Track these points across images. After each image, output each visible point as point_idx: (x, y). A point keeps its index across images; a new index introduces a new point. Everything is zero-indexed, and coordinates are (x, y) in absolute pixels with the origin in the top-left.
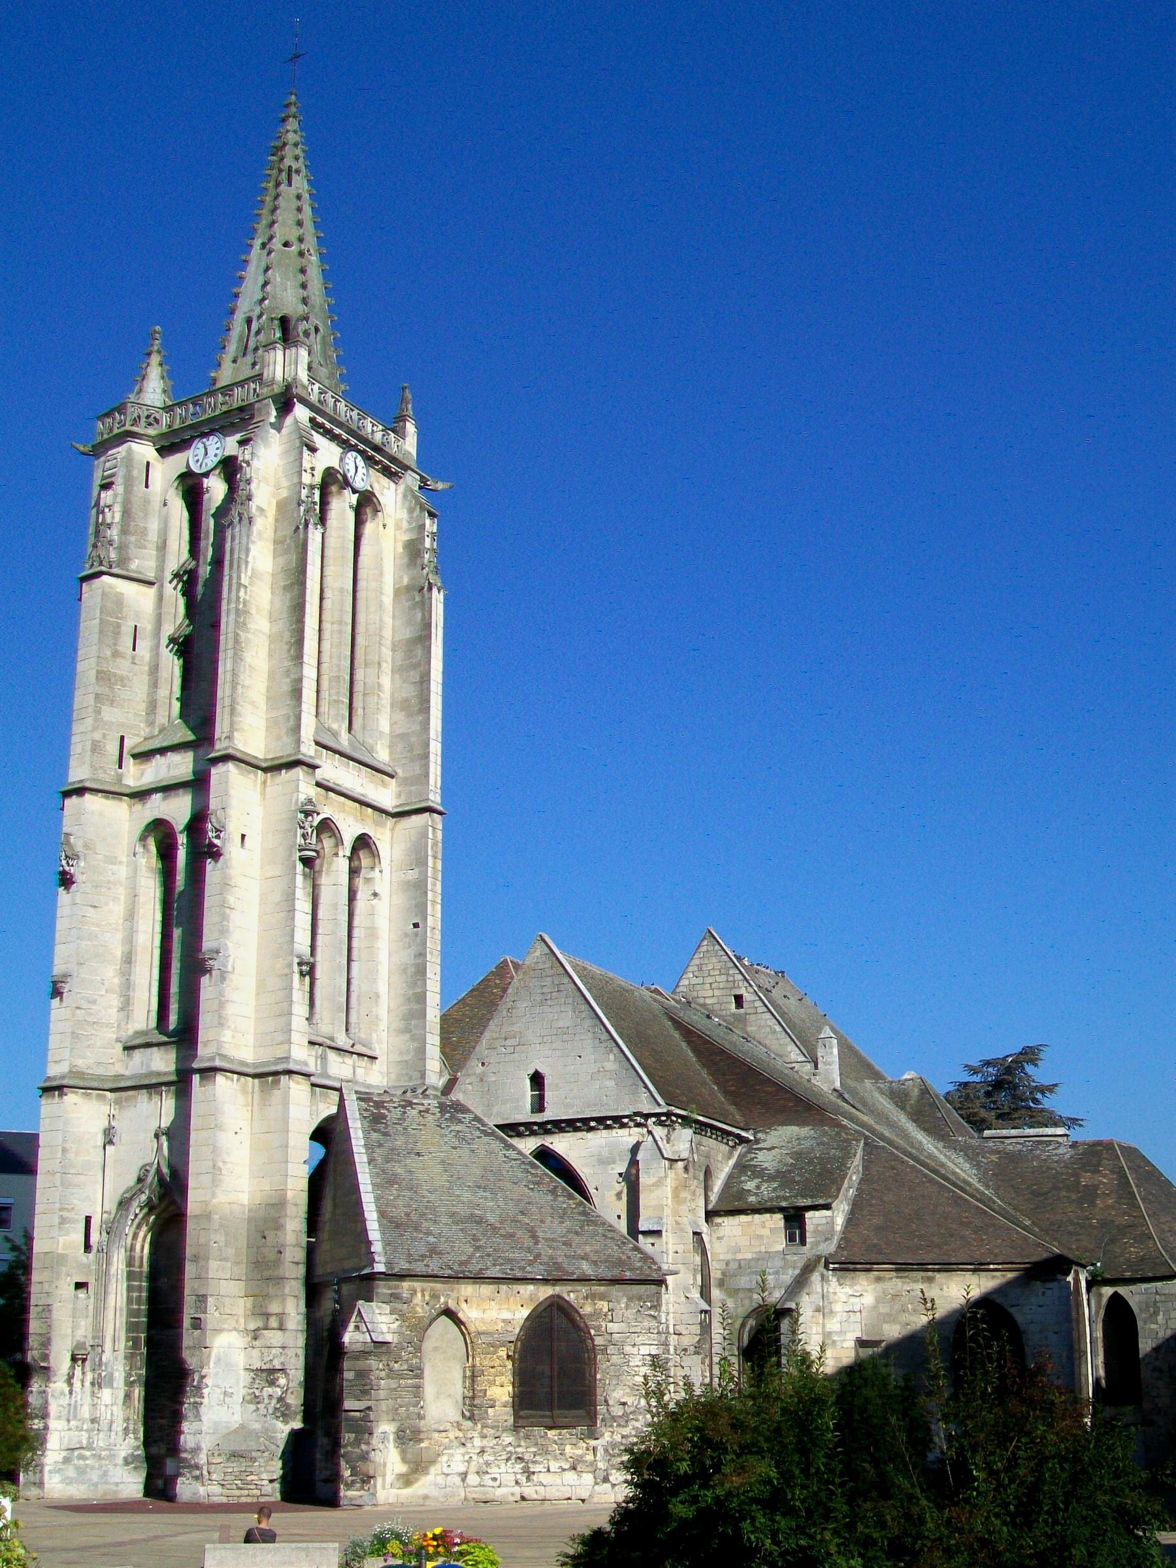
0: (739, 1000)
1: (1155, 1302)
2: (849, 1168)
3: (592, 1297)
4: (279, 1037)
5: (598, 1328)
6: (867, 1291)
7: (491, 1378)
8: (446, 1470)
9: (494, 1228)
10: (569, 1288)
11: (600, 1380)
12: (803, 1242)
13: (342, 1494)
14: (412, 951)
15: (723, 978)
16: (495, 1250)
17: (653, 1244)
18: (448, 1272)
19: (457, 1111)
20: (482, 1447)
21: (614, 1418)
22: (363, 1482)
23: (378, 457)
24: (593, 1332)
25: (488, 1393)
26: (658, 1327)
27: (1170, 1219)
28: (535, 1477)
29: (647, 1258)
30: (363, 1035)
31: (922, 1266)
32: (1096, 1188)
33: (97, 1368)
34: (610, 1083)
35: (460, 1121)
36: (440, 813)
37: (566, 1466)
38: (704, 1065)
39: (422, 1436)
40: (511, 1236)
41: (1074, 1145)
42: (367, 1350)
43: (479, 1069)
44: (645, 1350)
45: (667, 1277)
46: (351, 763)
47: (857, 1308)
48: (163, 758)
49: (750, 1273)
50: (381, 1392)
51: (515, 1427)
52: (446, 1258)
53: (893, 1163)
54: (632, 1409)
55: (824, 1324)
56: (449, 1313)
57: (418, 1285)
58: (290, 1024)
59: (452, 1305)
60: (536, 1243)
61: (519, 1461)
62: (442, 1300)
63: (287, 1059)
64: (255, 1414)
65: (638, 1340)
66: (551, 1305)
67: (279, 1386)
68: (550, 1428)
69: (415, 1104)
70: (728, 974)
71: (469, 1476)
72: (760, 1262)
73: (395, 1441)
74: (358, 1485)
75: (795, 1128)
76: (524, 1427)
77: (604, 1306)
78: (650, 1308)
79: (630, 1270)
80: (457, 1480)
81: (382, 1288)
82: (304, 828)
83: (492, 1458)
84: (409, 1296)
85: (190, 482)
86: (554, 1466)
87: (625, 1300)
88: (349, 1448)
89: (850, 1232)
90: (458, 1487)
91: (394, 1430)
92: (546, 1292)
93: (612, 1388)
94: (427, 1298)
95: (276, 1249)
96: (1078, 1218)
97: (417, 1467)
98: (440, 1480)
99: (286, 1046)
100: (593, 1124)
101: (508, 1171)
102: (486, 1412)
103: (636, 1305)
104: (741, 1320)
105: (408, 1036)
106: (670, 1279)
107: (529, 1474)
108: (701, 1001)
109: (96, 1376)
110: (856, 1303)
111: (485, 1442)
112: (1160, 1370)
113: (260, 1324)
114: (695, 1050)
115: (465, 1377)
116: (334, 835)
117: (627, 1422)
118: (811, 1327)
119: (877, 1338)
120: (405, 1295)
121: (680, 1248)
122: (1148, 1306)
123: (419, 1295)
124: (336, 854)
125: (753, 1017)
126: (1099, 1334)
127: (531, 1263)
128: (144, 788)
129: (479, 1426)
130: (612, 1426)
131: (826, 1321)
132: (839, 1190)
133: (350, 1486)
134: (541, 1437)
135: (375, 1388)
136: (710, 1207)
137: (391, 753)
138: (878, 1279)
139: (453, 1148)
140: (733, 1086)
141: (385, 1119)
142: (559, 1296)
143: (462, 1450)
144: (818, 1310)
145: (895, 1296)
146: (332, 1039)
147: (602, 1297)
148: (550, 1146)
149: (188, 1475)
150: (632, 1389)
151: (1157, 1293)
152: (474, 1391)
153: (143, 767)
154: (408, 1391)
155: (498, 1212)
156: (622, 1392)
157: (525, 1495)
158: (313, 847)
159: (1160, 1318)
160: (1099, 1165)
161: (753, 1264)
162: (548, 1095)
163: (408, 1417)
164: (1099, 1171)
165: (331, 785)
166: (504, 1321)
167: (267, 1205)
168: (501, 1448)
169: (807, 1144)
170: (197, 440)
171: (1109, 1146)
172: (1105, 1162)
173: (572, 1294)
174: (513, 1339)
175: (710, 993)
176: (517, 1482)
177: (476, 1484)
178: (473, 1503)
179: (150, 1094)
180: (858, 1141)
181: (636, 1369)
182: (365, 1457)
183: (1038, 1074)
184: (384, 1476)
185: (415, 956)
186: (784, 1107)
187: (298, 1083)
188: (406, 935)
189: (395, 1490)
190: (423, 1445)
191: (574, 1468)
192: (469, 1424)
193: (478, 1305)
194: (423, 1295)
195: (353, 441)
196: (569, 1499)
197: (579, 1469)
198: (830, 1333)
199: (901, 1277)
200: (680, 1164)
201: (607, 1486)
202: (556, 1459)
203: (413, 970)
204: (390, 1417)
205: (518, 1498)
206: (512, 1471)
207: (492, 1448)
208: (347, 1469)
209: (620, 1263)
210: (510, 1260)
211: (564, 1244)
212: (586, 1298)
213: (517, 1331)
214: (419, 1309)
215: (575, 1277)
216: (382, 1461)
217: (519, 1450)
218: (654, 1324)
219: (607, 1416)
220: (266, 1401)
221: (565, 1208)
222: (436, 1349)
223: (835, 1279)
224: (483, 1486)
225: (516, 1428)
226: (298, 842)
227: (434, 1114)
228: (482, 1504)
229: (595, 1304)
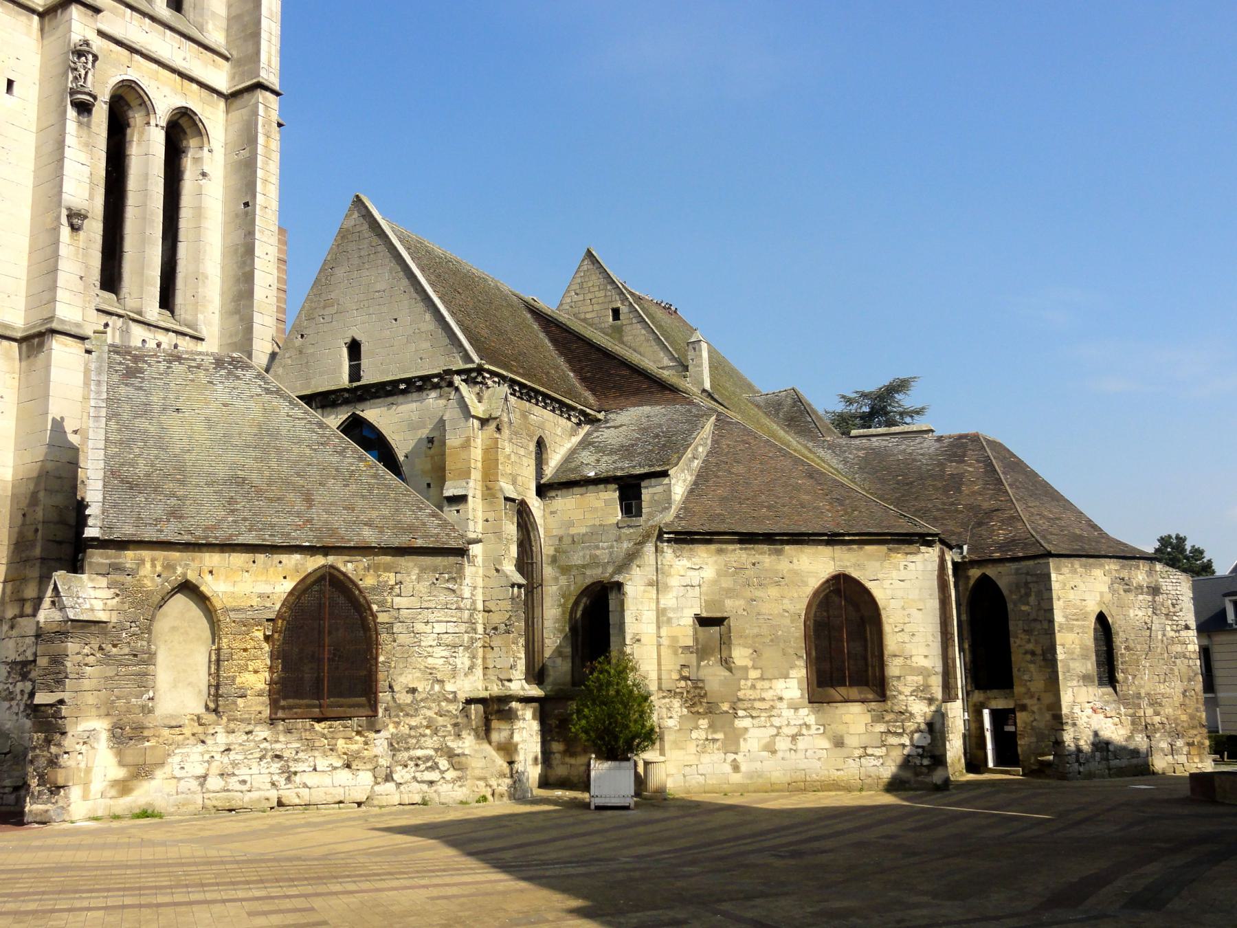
0: (616, 313)
1: (1026, 584)
2: (695, 438)
3: (377, 568)
4: (46, 296)
5: (382, 604)
6: (707, 564)
7: (242, 662)
8: (178, 773)
9: (259, 491)
10: (347, 558)
11: (383, 663)
12: (639, 514)
13: (27, 809)
14: (241, 233)
15: (602, 294)
16: (255, 514)
17: (458, 511)
18: (187, 538)
19: (236, 368)
20: (229, 744)
21: (400, 707)
22: (52, 792)
24: (375, 607)
25: (238, 680)
26: (457, 602)
27: (1038, 504)
28: (297, 779)
29: (445, 524)
30: (189, 317)
31: (769, 539)
32: (961, 476)
34: (426, 345)
35: (238, 378)
36: (277, 94)
37: (339, 763)
38: (561, 354)
39: (146, 734)
40: (279, 499)
41: (940, 439)
42: (63, 629)
44: (440, 628)
45: (471, 546)
46: (168, 32)
47: (695, 582)
49: (583, 548)
50: (86, 682)
51: (271, 719)
52: (187, 523)
53: (745, 438)
54: (424, 696)
55: (658, 599)
56: (188, 588)
57: (146, 554)
58: (55, 281)
59: (192, 576)
60: (310, 507)
61: (276, 760)
62: (179, 570)
63: (51, 319)
64: (8, 712)
65: (432, 617)
66: (322, 578)
68: (319, 720)
69: (185, 359)
70: (606, 289)
71: (209, 779)
72: (594, 537)
73: (109, 740)
74: (45, 797)
75: (649, 408)
76: (283, 720)
77: (391, 578)
78: (448, 581)
79: (425, 536)
80: (194, 785)
81: (97, 557)
82: (76, 69)
83: (240, 757)
84: (134, 566)
86: (322, 763)
87: (416, 571)
88: (38, 751)
89: (690, 502)
90: (194, 793)
91: (109, 727)
92: (318, 561)
93: (398, 671)
94: (159, 569)
95: (34, 527)
96: (944, 504)
97: (140, 772)
98: (171, 786)
101: (289, 431)
102: (235, 703)
103: (431, 577)
104: (574, 598)
105: (238, 316)
106: (475, 549)
107: (290, 775)
108: (582, 316)
110: (694, 577)
111: (232, 738)
112: (1033, 653)
114: (554, 341)
115: (210, 661)
116: (145, 102)
117: (416, 710)
118: (642, 602)
119: (718, 615)
120: (128, 565)
121: (491, 516)
122: (1018, 586)
123: (148, 565)
124: (148, 124)
125: (629, 328)
126: (964, 617)
127: (298, 528)
129: (225, 719)
130: (397, 716)
131: (660, 596)
132: (680, 459)
133: (36, 799)
134: (306, 730)
135: (70, 676)
136: (542, 482)
137: (228, 36)
138: (720, 551)
139: (225, 405)
140: (588, 372)
141: (143, 373)
142: (332, 567)
143: (201, 747)
144: (650, 584)
145: (739, 569)
146: (140, 313)
147: (388, 568)
148: (361, 414)
150: (424, 672)
151: (1027, 574)
152: (218, 676)
154: (129, 680)
155: (266, 473)
156: (410, 676)
157: (284, 800)
158: (86, 90)
159: (1032, 599)
160: (964, 456)
161: (586, 538)
162: (365, 362)
163: (129, 711)
164: (964, 461)
165: (137, 47)
166: (260, 596)
167: (28, 479)
168: (252, 744)
169: (656, 420)
171: (975, 439)
172: (969, 452)
173: (349, 565)
174: (272, 616)
175: (590, 308)
176: (273, 784)
177: (218, 789)
178: (213, 811)
180: (711, 416)
181: (429, 649)
182: (53, 762)
183: (906, 400)
184: (86, 784)
185: (245, 235)
186: (638, 389)
187: (66, 345)
188: (237, 216)
189: (108, 800)
190: (147, 744)
191: (348, 766)
192: (213, 716)
193: (227, 577)
194: (154, 566)
196: (341, 802)
197: (354, 767)
198: (665, 610)
199: (746, 549)
200: (493, 426)
201: (390, 786)
202: (325, 755)
203: (243, 249)
204: (103, 711)
205: (275, 804)
206: (267, 771)
207: (241, 745)
208: (34, 777)
209: (411, 529)
210: (273, 526)
211: (344, 508)
212: (368, 569)
213: (277, 607)
214: (147, 582)
215: (352, 544)
216: (83, 765)
217: (278, 746)
218: (452, 598)
219: (391, 703)
220: (19, 697)
221: (353, 471)
222: (174, 629)
223: (670, 551)
224: (228, 790)
225: (272, 721)
226: (70, 85)
227: (207, 370)
228: (227, 813)
229: (379, 576)
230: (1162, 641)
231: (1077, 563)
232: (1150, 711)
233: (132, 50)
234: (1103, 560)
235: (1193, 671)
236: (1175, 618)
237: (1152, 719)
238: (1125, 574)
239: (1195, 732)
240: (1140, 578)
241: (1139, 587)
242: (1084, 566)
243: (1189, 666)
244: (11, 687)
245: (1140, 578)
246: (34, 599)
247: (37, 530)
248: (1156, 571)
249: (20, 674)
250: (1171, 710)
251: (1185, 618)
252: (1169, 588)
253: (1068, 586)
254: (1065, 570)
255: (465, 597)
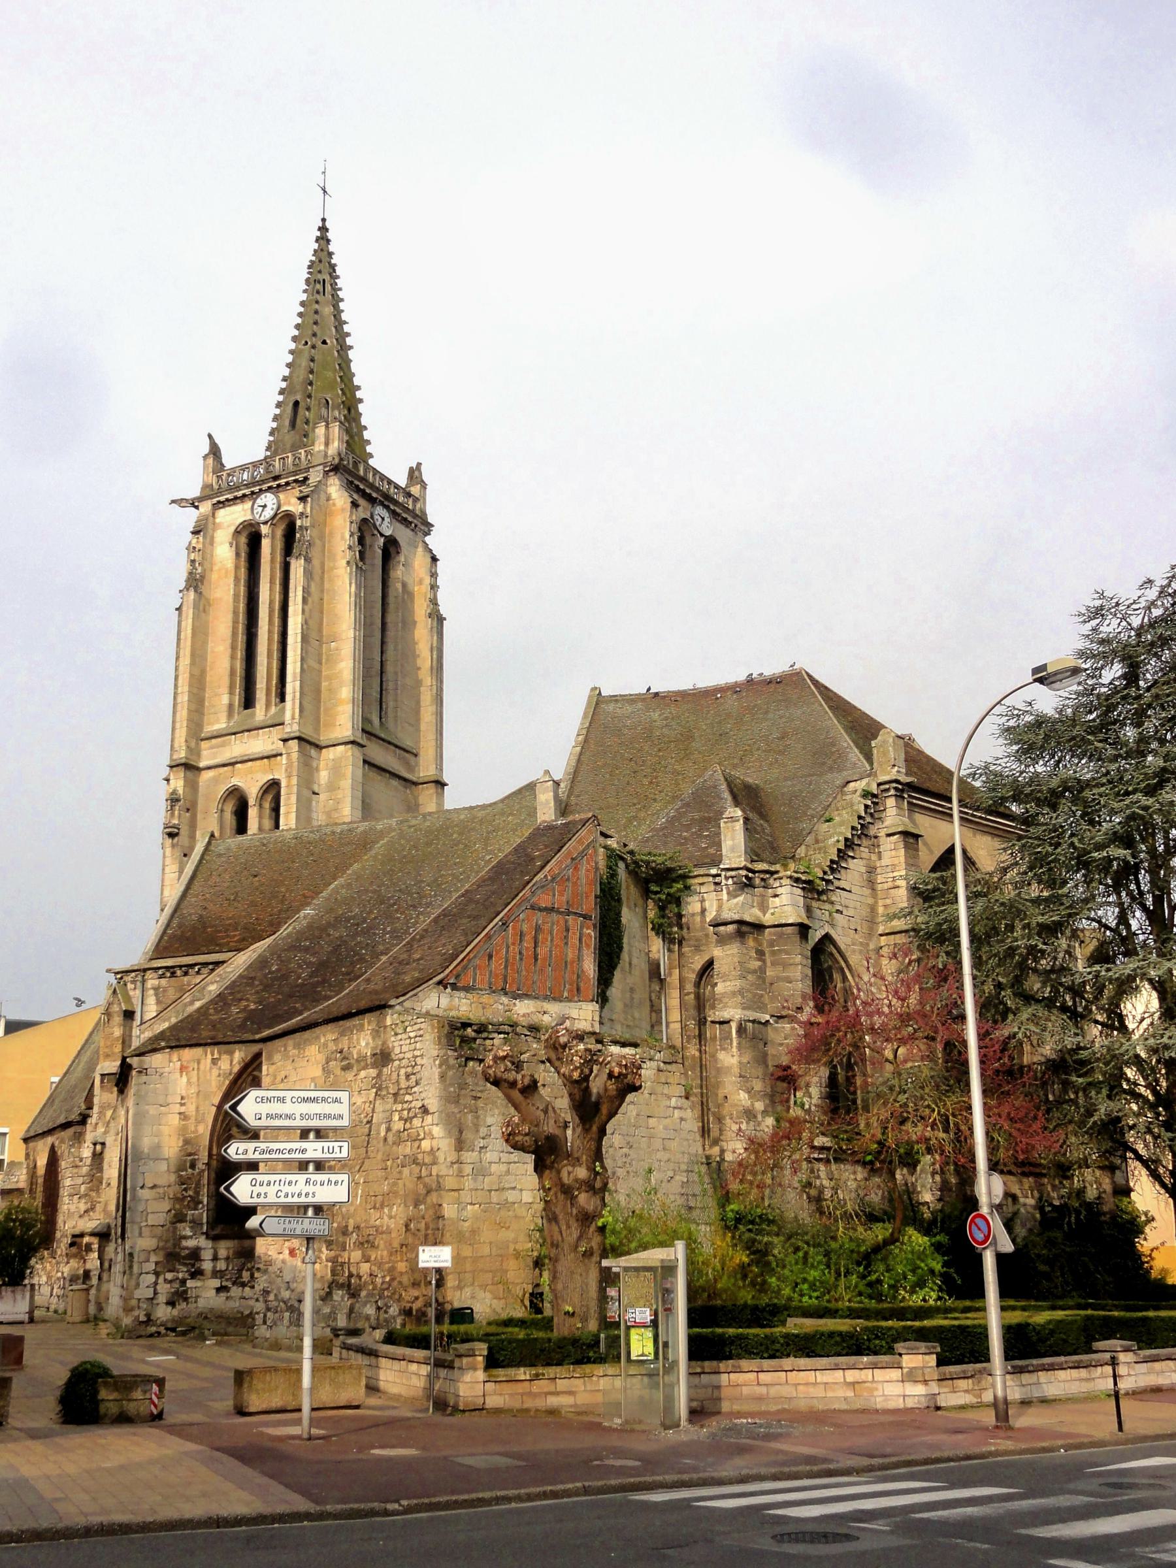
23: (282, 481)
46: (261, 731)
195: (256, 489)
230: (385, 1139)
231: (290, 1041)
232: (356, 1255)
233: (233, 764)
234: (318, 1030)
235: (425, 1185)
236: (408, 1098)
237: (358, 1268)
238: (344, 1043)
239: (416, 1293)
240: (363, 1044)
241: (361, 1059)
242: (297, 1046)
243: (420, 1178)
245: (363, 1044)
248: (385, 1027)
250: (385, 1253)
251: (423, 1095)
252: (405, 1049)
253: (279, 1079)
254: (277, 1057)
255: (85, 1156)
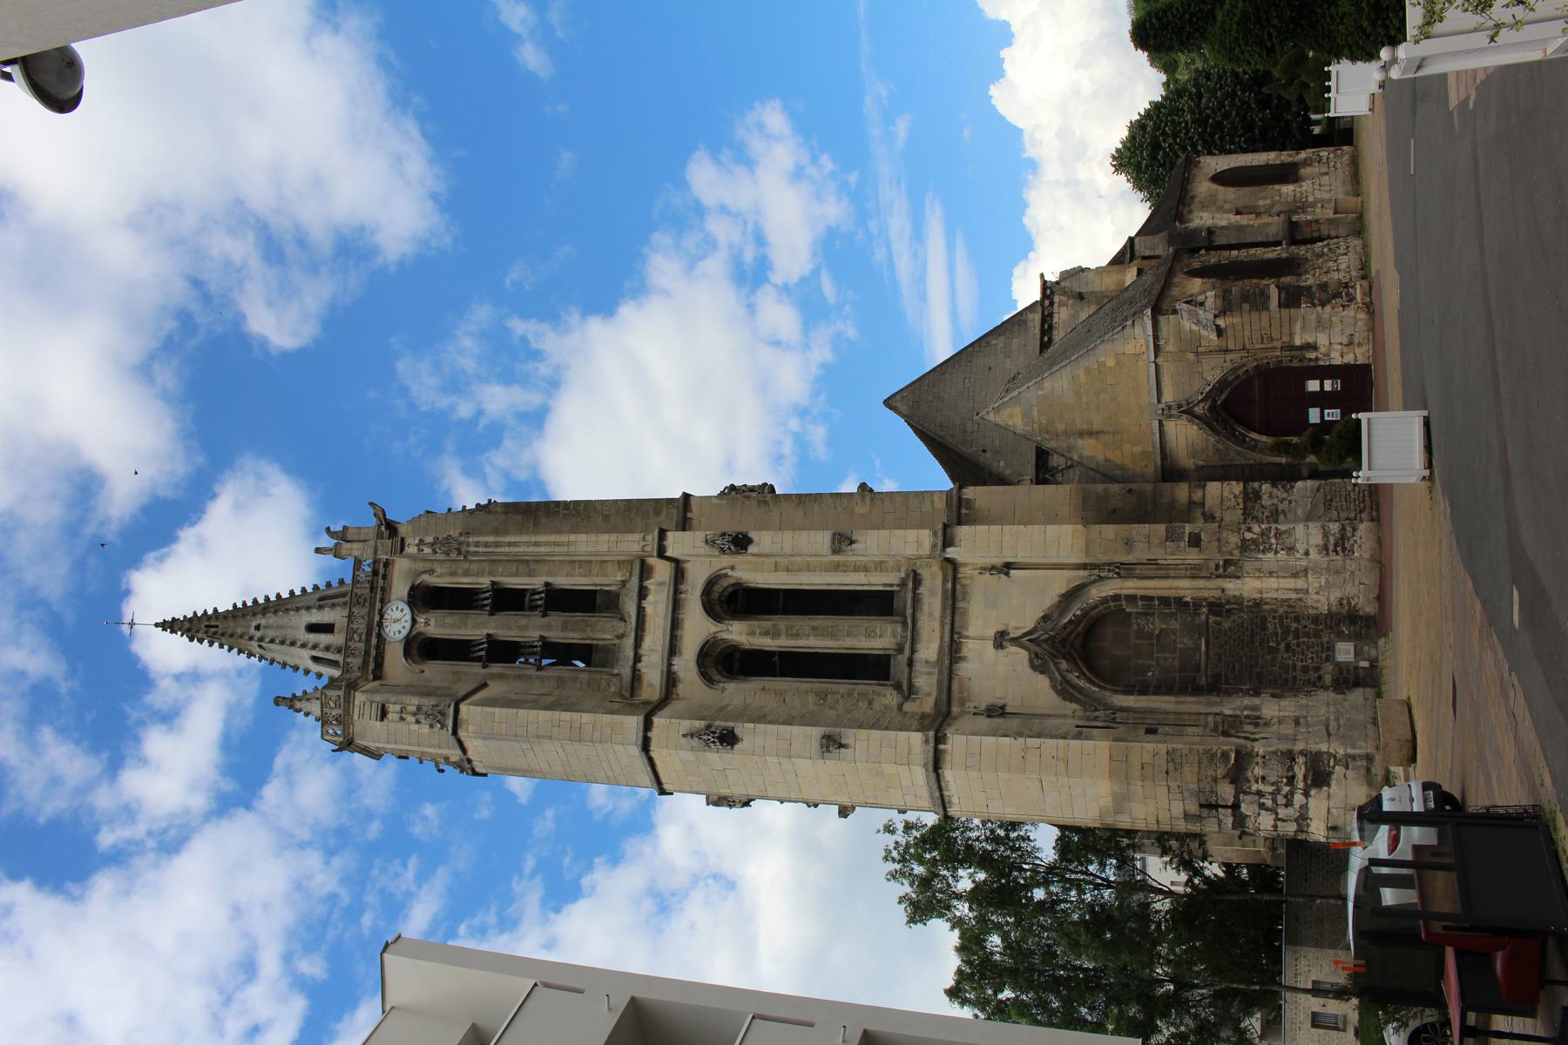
33: (1238, 719)
43: (988, 455)
48: (643, 658)
64: (1288, 516)
67: (1260, 487)
85: (415, 645)
99: (936, 497)
100: (1046, 339)
109: (1248, 721)
113: (1198, 513)
128: (664, 683)
149: (1351, 541)
153: (645, 684)
170: (382, 631)
179: (960, 658)
220: (1275, 501)
244: (1266, 514)
246: (1190, 488)
247: (1130, 490)
249: (1255, 501)
